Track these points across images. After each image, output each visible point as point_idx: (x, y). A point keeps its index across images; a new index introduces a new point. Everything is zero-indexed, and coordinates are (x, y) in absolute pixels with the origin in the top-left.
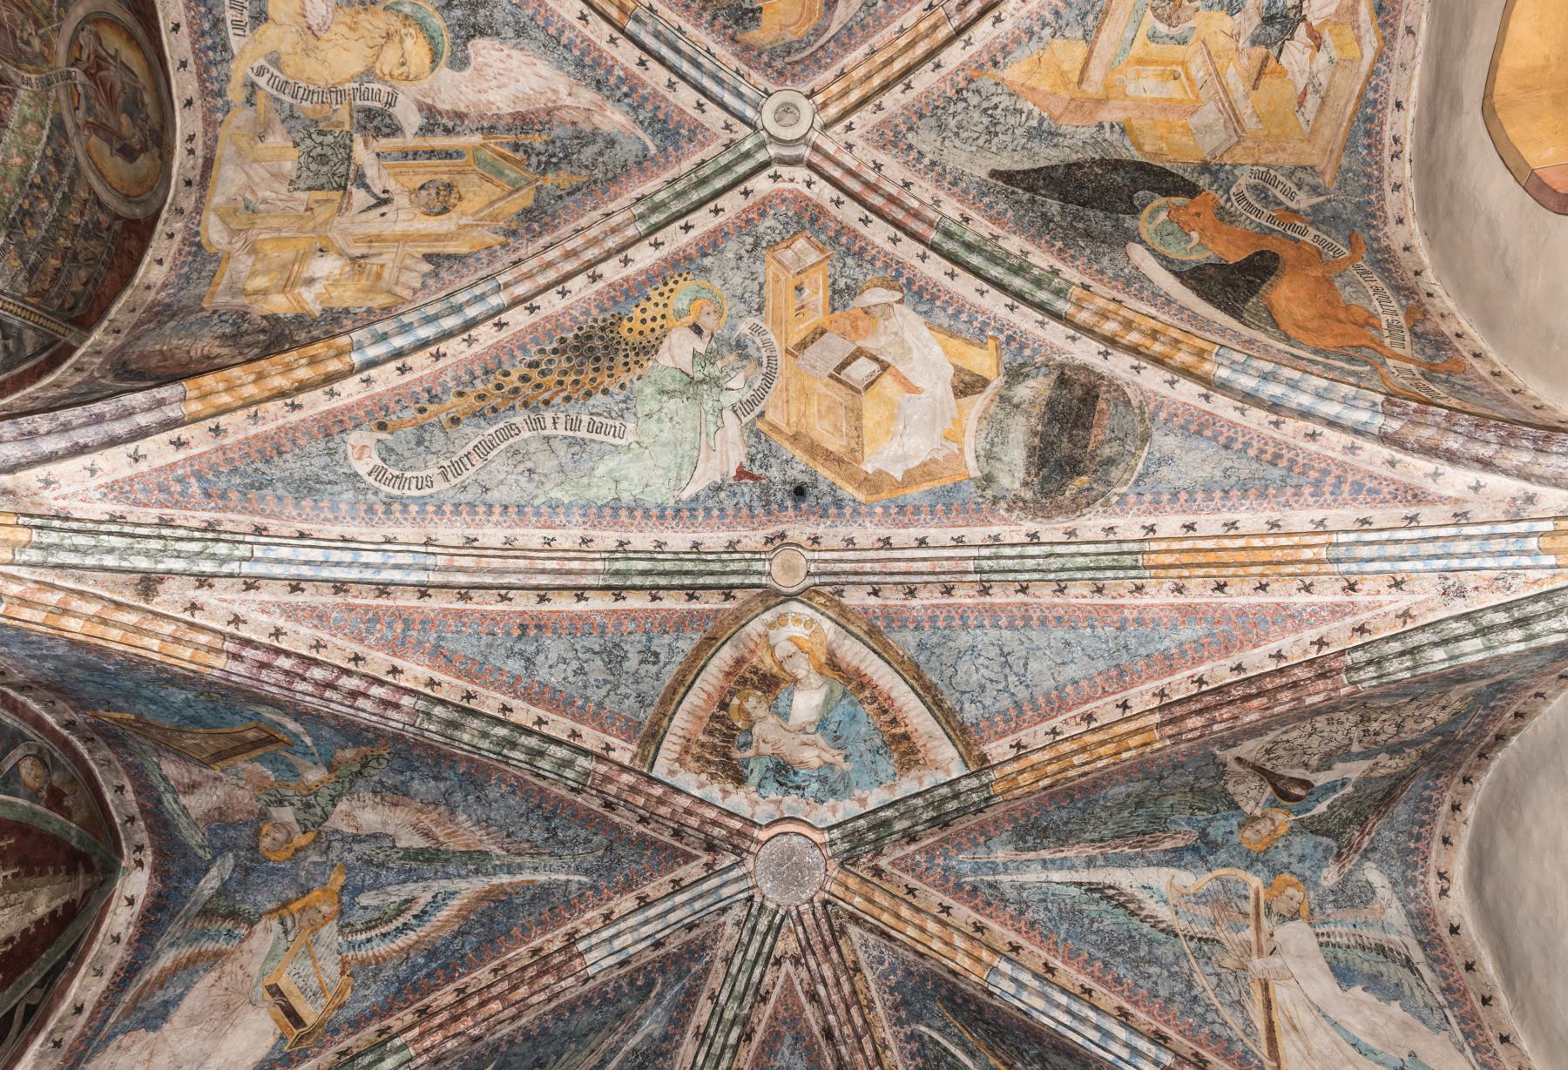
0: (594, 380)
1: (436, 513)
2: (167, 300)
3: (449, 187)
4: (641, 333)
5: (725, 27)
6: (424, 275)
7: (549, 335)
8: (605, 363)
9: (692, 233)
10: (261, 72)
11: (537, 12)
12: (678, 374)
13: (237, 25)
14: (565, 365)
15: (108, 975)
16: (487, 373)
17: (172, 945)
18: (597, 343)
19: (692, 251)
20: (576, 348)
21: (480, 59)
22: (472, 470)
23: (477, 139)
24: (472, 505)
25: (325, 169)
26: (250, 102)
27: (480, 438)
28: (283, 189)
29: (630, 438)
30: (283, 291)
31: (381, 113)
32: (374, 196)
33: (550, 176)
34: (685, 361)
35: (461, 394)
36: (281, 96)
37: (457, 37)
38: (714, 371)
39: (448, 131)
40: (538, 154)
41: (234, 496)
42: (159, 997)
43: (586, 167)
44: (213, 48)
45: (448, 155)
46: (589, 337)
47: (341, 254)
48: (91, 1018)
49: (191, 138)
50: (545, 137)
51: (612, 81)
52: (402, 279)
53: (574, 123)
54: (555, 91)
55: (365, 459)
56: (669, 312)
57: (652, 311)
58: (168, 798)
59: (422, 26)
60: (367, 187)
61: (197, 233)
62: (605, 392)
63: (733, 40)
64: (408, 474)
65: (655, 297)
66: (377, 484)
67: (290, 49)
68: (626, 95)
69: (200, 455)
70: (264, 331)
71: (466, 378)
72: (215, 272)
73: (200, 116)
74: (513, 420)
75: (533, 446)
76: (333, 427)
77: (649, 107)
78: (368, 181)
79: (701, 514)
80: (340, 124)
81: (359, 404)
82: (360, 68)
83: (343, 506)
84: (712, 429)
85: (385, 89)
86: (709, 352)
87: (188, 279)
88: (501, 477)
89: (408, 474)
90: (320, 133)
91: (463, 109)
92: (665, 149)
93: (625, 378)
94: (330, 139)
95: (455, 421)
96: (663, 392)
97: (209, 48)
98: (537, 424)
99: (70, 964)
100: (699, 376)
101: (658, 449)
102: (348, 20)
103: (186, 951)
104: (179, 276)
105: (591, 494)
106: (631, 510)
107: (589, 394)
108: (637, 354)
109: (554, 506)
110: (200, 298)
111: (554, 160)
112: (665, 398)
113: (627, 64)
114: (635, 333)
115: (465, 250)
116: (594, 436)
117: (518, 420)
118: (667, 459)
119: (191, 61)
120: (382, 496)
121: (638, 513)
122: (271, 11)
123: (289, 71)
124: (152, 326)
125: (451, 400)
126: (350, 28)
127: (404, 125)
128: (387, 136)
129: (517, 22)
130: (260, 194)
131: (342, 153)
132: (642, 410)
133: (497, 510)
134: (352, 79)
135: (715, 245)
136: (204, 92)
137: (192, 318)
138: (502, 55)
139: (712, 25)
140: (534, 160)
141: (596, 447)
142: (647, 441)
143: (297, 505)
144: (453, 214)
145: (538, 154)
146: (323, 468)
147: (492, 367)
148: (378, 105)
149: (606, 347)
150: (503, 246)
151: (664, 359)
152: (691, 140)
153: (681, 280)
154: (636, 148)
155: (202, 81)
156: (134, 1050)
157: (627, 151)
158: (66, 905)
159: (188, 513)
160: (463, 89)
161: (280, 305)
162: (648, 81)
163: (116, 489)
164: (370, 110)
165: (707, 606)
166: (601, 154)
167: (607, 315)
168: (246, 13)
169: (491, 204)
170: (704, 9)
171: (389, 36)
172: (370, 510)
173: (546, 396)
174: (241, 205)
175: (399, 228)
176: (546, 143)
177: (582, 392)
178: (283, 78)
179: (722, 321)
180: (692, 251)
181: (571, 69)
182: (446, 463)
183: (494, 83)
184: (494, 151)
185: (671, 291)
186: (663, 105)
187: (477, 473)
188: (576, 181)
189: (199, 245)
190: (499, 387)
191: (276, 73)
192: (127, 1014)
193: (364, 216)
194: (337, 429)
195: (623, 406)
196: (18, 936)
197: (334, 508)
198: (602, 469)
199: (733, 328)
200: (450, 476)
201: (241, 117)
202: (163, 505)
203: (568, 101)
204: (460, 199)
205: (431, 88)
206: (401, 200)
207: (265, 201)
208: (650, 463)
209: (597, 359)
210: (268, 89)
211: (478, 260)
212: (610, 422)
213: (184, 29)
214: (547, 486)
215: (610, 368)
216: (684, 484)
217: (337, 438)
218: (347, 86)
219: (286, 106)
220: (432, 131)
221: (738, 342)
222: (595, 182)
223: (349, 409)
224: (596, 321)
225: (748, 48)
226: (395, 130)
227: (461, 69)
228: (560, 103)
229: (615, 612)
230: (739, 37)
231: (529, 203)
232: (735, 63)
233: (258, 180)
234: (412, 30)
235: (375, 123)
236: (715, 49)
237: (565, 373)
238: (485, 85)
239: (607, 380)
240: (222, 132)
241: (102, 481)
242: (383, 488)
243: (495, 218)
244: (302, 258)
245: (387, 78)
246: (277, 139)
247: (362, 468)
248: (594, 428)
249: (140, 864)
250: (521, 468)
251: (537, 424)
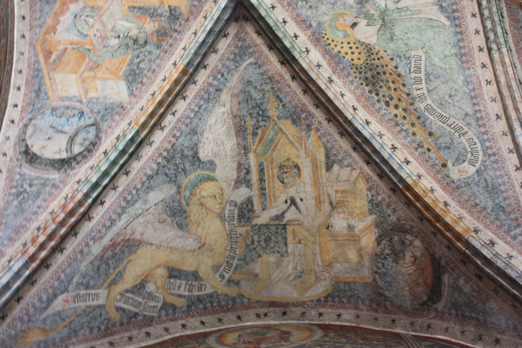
0: (390, 74)
1: (487, 134)
2: (368, 303)
3: (281, 167)
4: (360, 53)
5: (181, 25)
6: (342, 167)
7: (368, 99)
8: (380, 69)
9: (298, 34)
10: (222, 277)
11: (184, 123)
12: (381, 32)
13: (200, 289)
14: (384, 89)
16: (397, 125)
18: (369, 74)
19: (309, 32)
20: (374, 84)
21: (210, 155)
22: (457, 122)
23: (251, 156)
24: (477, 119)
25: (273, 238)
26: (237, 283)
27: (437, 121)
28: (287, 259)
29: (420, 52)
30: (359, 240)
31: (241, 210)
32: (289, 208)
33: (271, 113)
34: (373, 30)
35: (414, 134)
36: (234, 265)
37: (199, 166)
38: (376, 14)
39: (248, 172)
40: (258, 121)
41: (513, 216)
43: (264, 95)
44: (212, 303)
45: (261, 171)
46: (366, 79)
47: (330, 216)
49: (258, 316)
50: (248, 119)
51: (215, 83)
52: (345, 178)
53: (239, 103)
54: (223, 114)
55: (466, 169)
56: (345, 41)
57: (346, 49)
59: (195, 186)
60: (284, 213)
61: (319, 300)
62: (396, 67)
63: (187, 20)
64: (469, 150)
65: (336, 50)
66: (479, 162)
67: (211, 260)
68: (223, 75)
69: (495, 234)
70: (390, 240)
71: (403, 133)
72: (345, 283)
73: (246, 311)
74: (423, 108)
75: (435, 97)
76: (452, 187)
77: (228, 63)
78: (279, 213)
79: (456, 14)
80: (247, 232)
81: (434, 177)
82: (218, 222)
83: (498, 173)
84: (409, 12)
85: (228, 207)
86: (366, 17)
87: (351, 296)
88: (457, 109)
89: (469, 150)
90: (253, 243)
91: (235, 165)
92: (251, 53)
93: (387, 59)
94: (256, 237)
95: (431, 134)
96: (392, 39)
97: (212, 305)
98: (422, 98)
100: (380, 22)
101: (424, 39)
102: (195, 226)
105: (456, 68)
106: (460, 48)
107: (399, 75)
108: (372, 54)
109: (467, 82)
110: (366, 285)
111: (261, 113)
112: (395, 38)
113: (206, 76)
114: (360, 56)
115: (322, 150)
116: (423, 70)
117: (422, 106)
118: (430, 34)
119: (218, 316)
120: (485, 159)
121: (462, 44)
122: (193, 269)
123: (221, 261)
124: (388, 304)
125: (418, 138)
126: (198, 226)
127: (246, 196)
128: (252, 205)
129: (190, 134)
130: (291, 272)
131: (264, 229)
132: (404, 48)
133: (477, 108)
134: (224, 225)
135: (304, 21)
136: (233, 309)
137: (381, 284)
138: (207, 142)
139: (180, 32)
140: (262, 124)
141: (428, 69)
142: (421, 44)
143: (506, 191)
144: (299, 162)
145: (258, 121)
146: (478, 186)
147: (395, 123)
148: (236, 211)
149: (371, 70)
150: (318, 130)
151: (372, 40)
152: (245, 40)
153: (326, 37)
154: (251, 69)
155: (228, 310)
157: (253, 74)
160: (225, 164)
161: (368, 240)
162: (214, 63)
164: (239, 215)
165: (504, 9)
166: (255, 88)
167: (352, 71)
168: (194, 283)
169: (291, 142)
170: (171, 37)
171: (201, 204)
172: (496, 162)
173: (404, 96)
174: (298, 281)
175: (309, 189)
176: (251, 118)
177: (398, 79)
178: (225, 264)
179: (348, 13)
180: (309, 32)
181: (211, 105)
182: (457, 134)
183: (221, 147)
184: (258, 146)
185: (333, 41)
186: (226, 56)
187: (459, 120)
188: (272, 99)
189: (326, 298)
190: (404, 118)
191: (222, 268)
193: (303, 210)
194: (453, 185)
195: (403, 58)
197: (501, 176)
198: (440, 64)
199: (351, 7)
200: (463, 131)
201: (247, 289)
203: (228, 106)
204: (288, 160)
205: (226, 181)
206: (292, 192)
207: (295, 268)
208: (432, 42)
209: (378, 73)
210: (231, 273)
211: (328, 142)
212: (413, 63)
213: (203, 319)
214: (456, 87)
215: (382, 66)
216: (441, 24)
217: (458, 183)
218: (228, 228)
219: (239, 262)
220: (249, 181)
221: (359, 4)
222: (273, 88)
223: (438, 182)
224: (356, 77)
225: (191, 12)
226: (249, 201)
227: (215, 165)
228: (229, 111)
229: (517, 51)
230: (186, 17)
231: (289, 121)
232: (200, 18)
233: (281, 275)
234: (198, 191)
235: (246, 212)
236: (192, 30)
237: (389, 88)
238: (223, 152)
239: (389, 67)
240: (254, 298)
242: (480, 158)
243: (301, 139)
244: (334, 237)
245: (222, 206)
246: (257, 267)
247: (472, 170)
248: (418, 70)
250: (450, 100)
251: (422, 98)
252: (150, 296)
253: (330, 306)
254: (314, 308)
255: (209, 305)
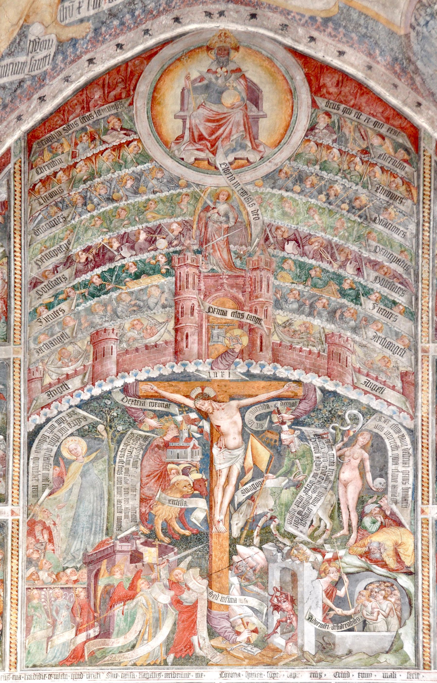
44: (132, 12)
61: (313, 19)
73: (188, 9)
87: (365, 36)
97: (133, 15)
104: (360, 42)
110: (392, 33)
119: (144, 27)
155: (160, 13)
189: (326, 20)
252: (36, 43)
253: (330, 35)
254: (303, 25)
255: (128, 16)
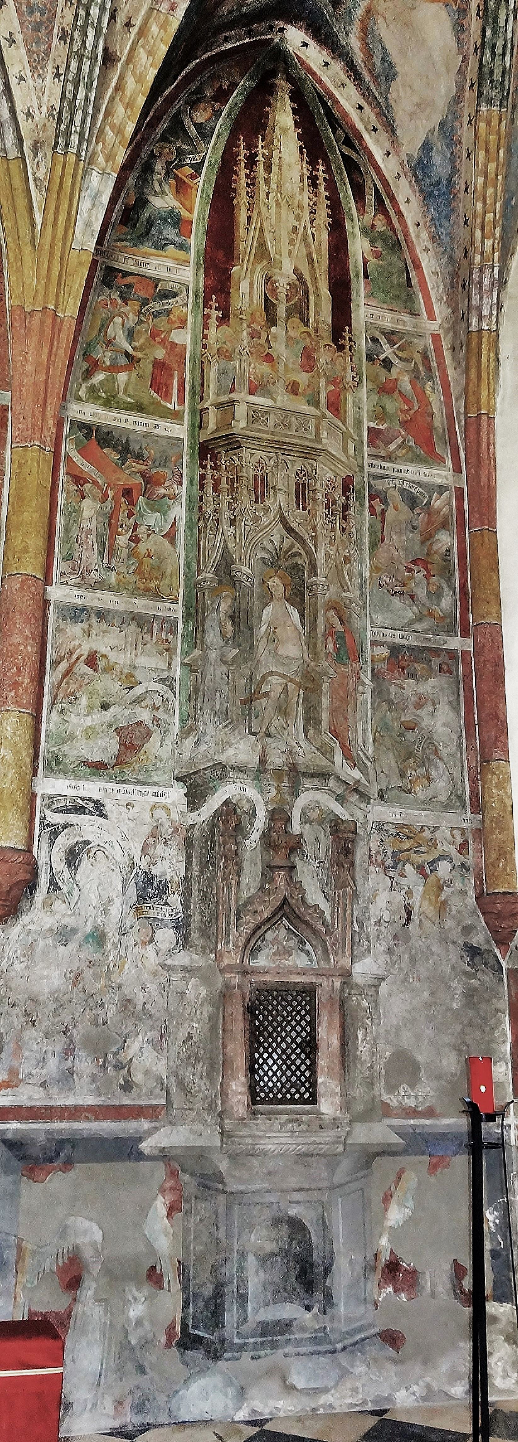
15: (347, 81)
17: (347, 35)
42: (377, 60)
48: (369, 104)
58: (245, 10)
99: (330, 103)
103: (355, 29)
156: (402, 93)
158: (292, 99)
159: (58, 14)
163: (37, 64)
192: (378, 85)
196: (301, 143)
202: (50, 33)
241: (29, 74)
249: (282, 30)
